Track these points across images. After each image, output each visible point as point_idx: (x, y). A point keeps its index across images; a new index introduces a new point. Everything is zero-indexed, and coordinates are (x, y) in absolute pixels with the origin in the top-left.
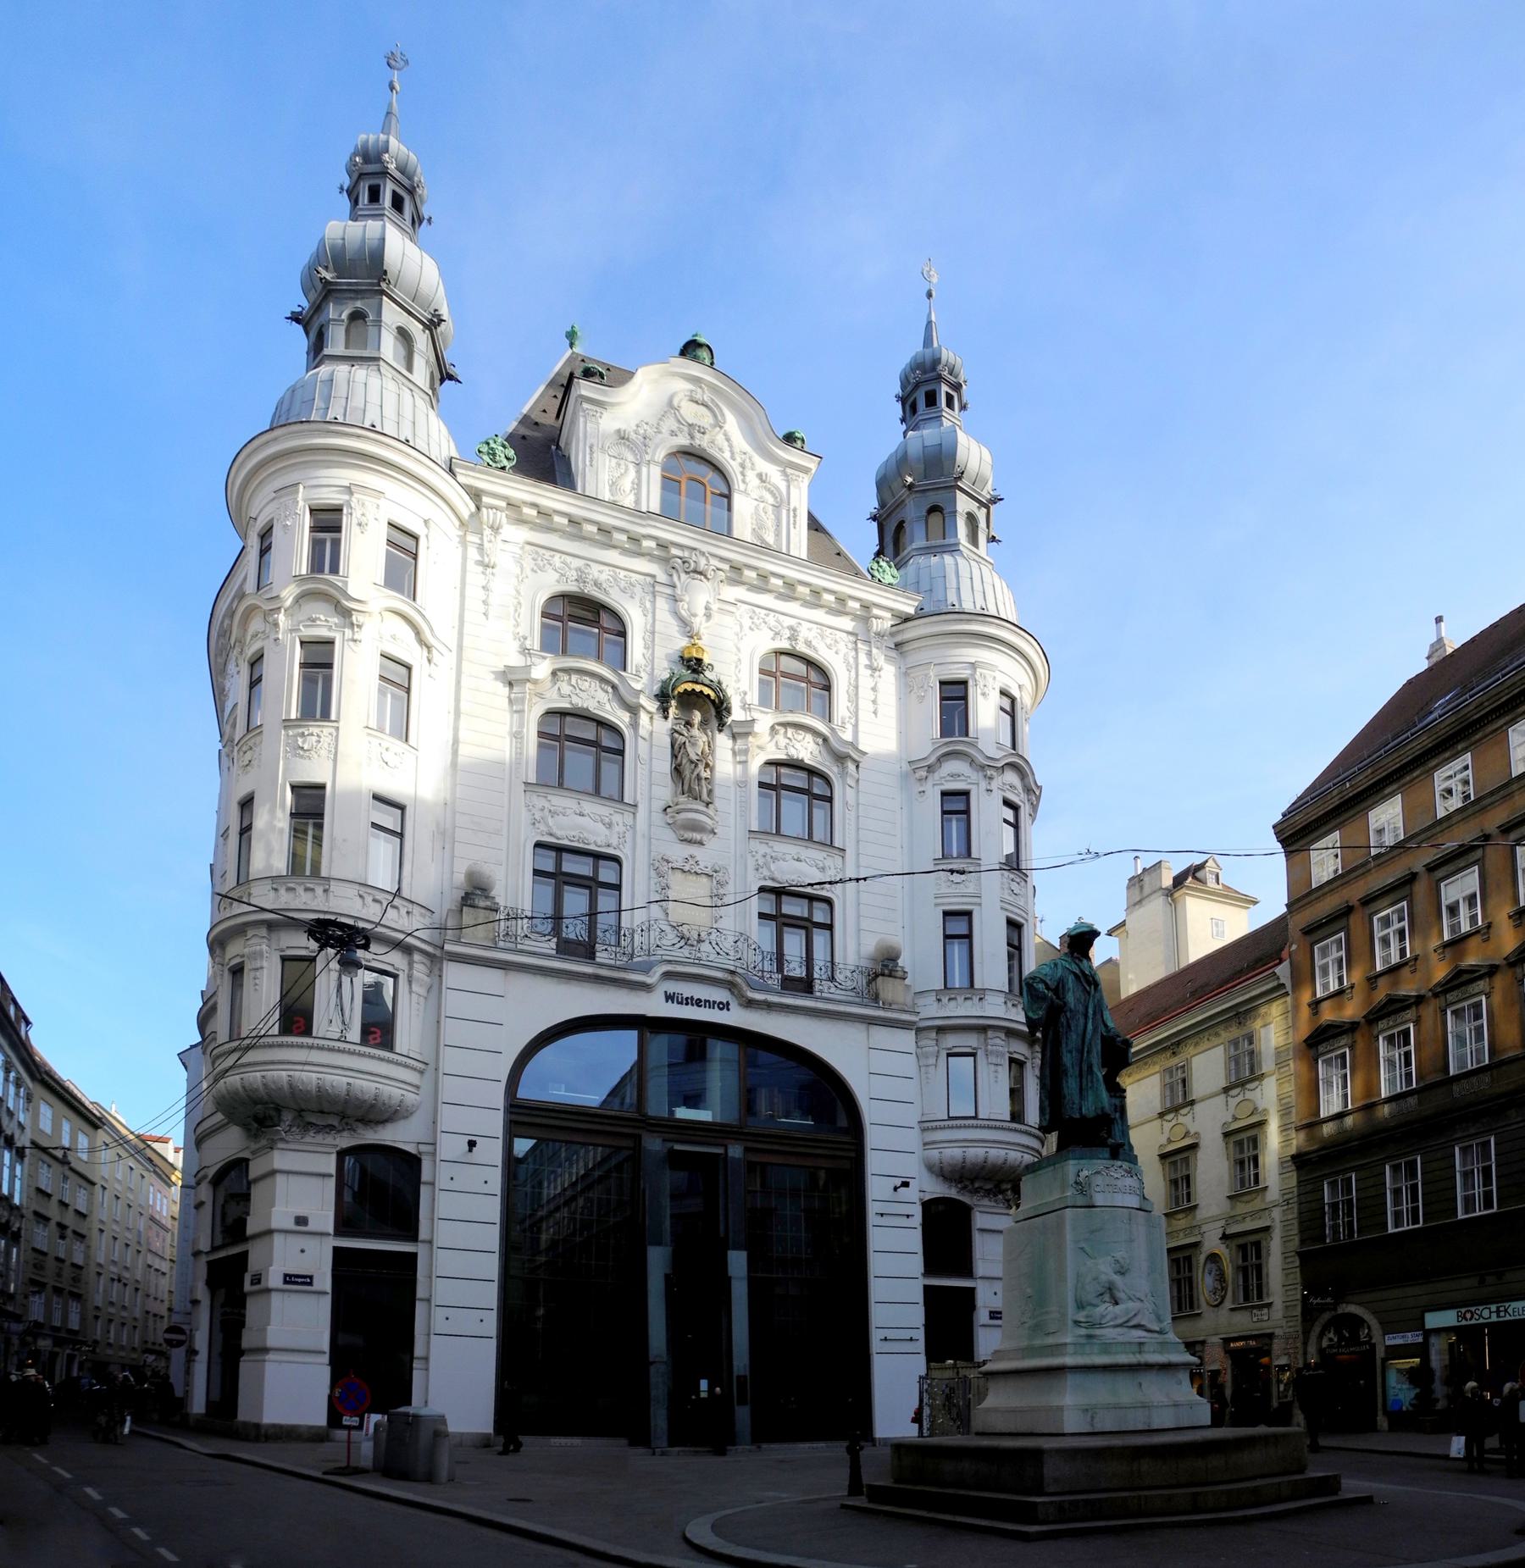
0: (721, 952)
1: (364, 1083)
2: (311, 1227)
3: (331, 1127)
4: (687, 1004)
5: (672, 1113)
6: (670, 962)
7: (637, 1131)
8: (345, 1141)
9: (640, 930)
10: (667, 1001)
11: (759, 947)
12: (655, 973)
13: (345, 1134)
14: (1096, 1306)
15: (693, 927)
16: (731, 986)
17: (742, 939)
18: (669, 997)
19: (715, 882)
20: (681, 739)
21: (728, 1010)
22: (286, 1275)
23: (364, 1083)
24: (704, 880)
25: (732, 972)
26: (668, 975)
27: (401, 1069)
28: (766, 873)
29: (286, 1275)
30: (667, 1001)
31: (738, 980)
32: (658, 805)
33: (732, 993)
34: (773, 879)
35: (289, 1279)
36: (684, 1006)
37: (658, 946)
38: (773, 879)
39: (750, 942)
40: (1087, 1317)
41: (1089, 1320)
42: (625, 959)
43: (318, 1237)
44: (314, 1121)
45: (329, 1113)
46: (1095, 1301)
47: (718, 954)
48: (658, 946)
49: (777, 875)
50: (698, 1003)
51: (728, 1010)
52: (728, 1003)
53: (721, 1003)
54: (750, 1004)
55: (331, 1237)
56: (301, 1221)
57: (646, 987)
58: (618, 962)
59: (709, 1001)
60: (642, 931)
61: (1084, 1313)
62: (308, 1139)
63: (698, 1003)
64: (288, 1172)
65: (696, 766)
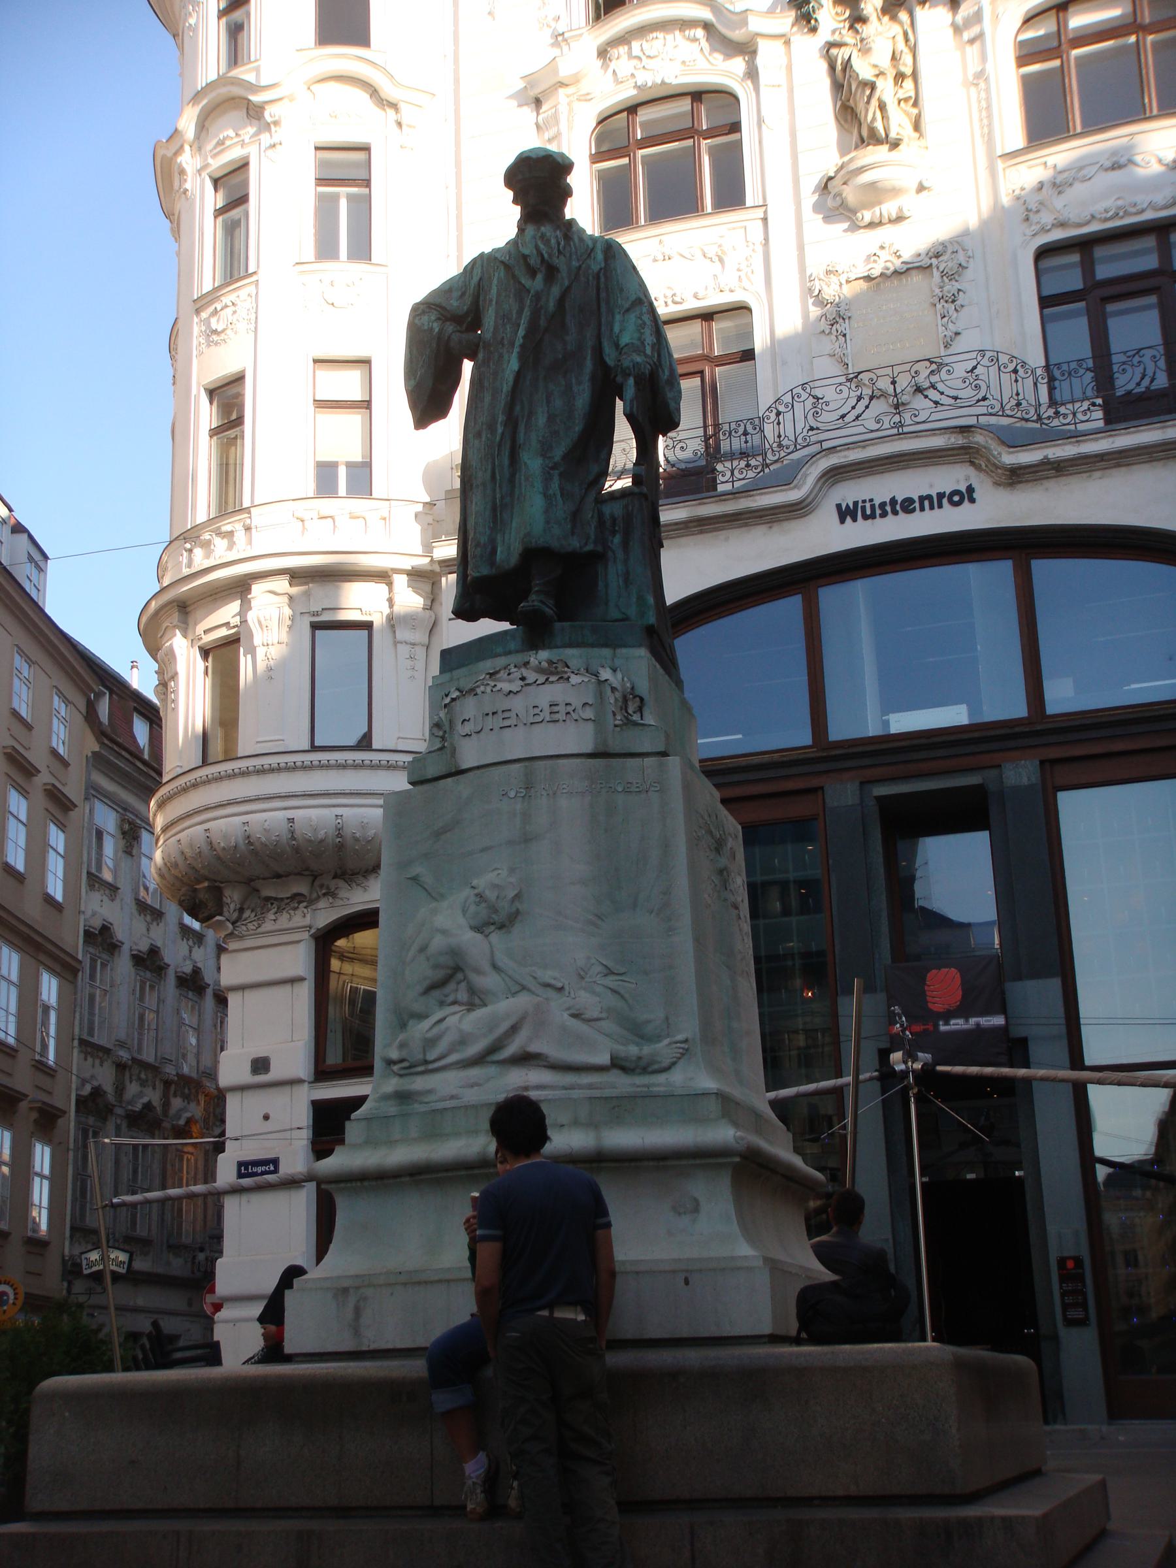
0: (944, 400)
1: (314, 813)
2: (274, 1074)
3: (297, 898)
4: (884, 515)
5: (886, 724)
6: (832, 450)
7: (814, 782)
8: (325, 915)
9: (773, 416)
10: (842, 521)
11: (1024, 364)
12: (806, 476)
13: (322, 904)
14: (422, 1017)
15: (879, 372)
16: (967, 454)
17: (985, 362)
18: (846, 513)
19: (936, 274)
20: (841, 54)
21: (972, 500)
22: (240, 1164)
23: (314, 813)
24: (916, 278)
25: (964, 429)
26: (835, 475)
27: (382, 774)
28: (1047, 218)
29: (240, 1164)
30: (842, 521)
31: (979, 438)
32: (810, 184)
33: (978, 468)
34: (1062, 225)
35: (245, 1168)
36: (878, 520)
37: (812, 429)
38: (1062, 225)
39: (1003, 359)
40: (402, 1046)
41: (404, 1054)
42: (751, 474)
43: (287, 1089)
44: (273, 895)
45: (287, 876)
46: (418, 1007)
47: (936, 403)
48: (812, 429)
49: (1073, 215)
50: (907, 506)
51: (972, 500)
52: (970, 490)
53: (956, 492)
54: (1016, 477)
55: (306, 1085)
56: (260, 1065)
57: (796, 510)
58: (737, 484)
59: (929, 497)
60: (778, 414)
61: (401, 1037)
62: (268, 926)
63: (907, 506)
64: (242, 988)
65: (873, 86)
